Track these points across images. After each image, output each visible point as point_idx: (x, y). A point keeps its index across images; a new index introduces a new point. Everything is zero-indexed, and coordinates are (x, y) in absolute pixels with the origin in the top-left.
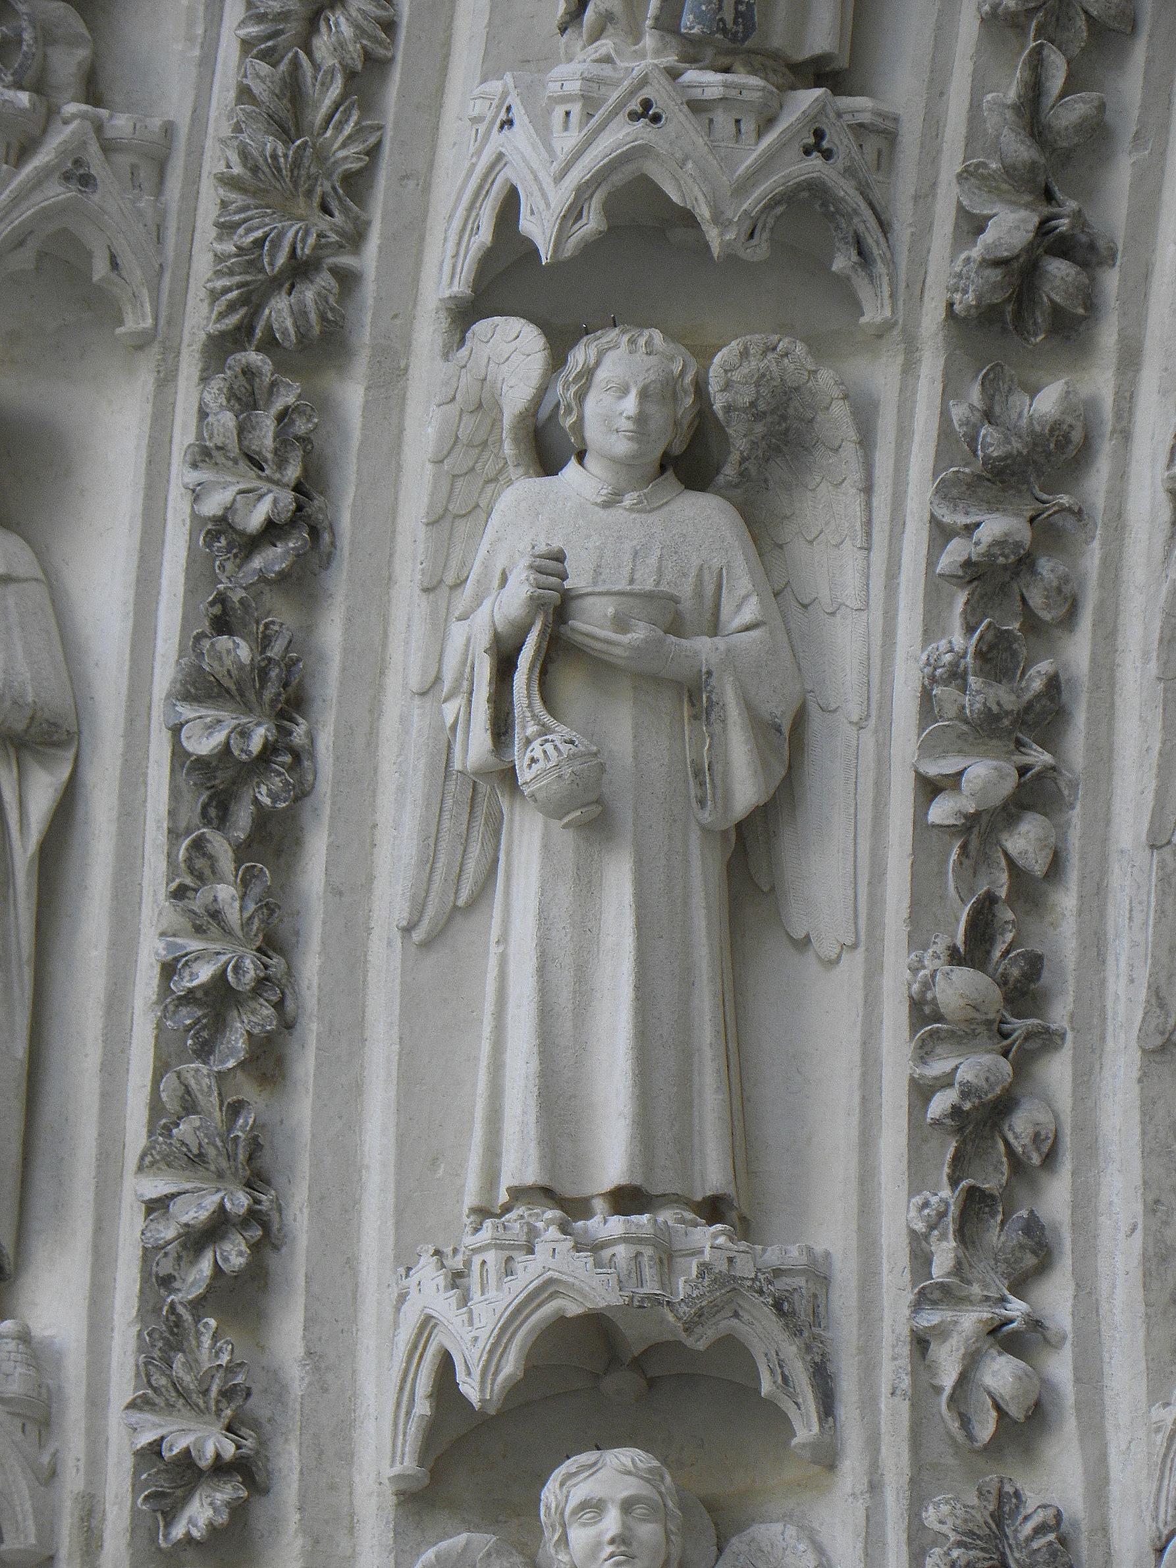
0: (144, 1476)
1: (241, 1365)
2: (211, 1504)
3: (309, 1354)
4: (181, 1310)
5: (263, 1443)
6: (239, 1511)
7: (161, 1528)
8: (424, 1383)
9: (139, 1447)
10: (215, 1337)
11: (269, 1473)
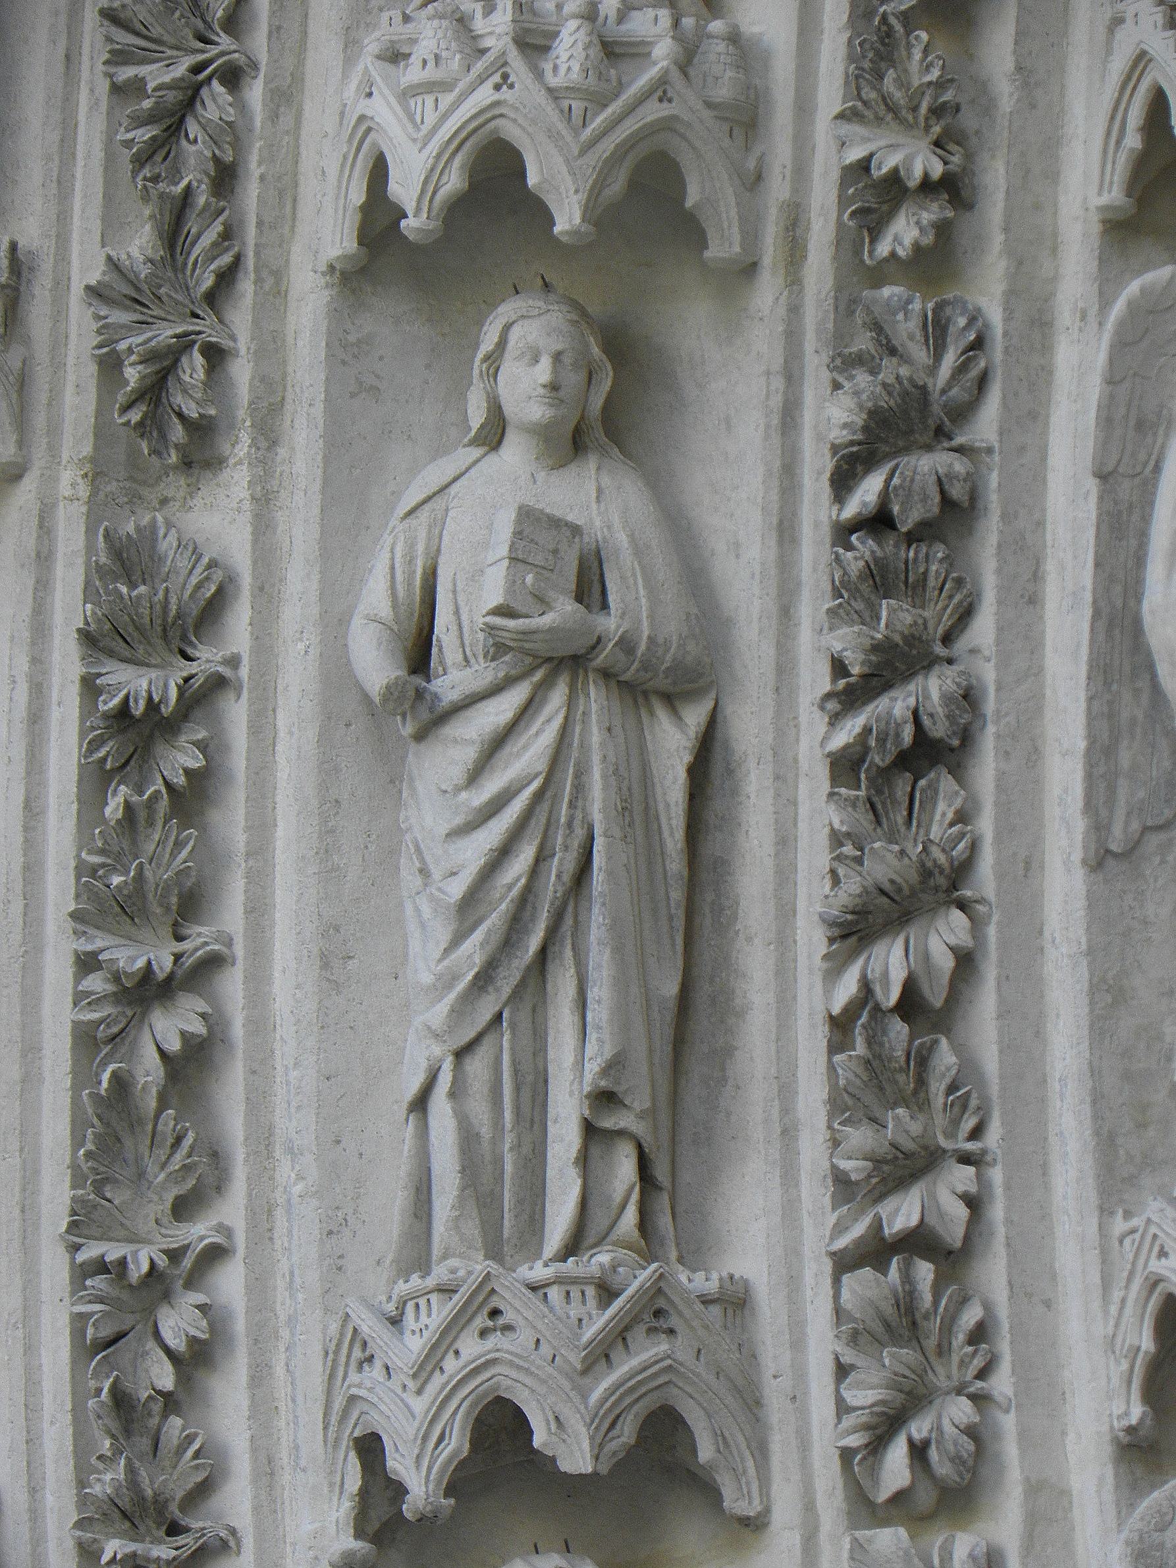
0: (851, 191)
1: (952, 80)
2: (917, 223)
3: (1019, 69)
4: (893, 21)
5: (969, 157)
6: (943, 230)
7: (867, 245)
8: (1136, 115)
9: (848, 162)
10: (926, 52)
11: (974, 188)
